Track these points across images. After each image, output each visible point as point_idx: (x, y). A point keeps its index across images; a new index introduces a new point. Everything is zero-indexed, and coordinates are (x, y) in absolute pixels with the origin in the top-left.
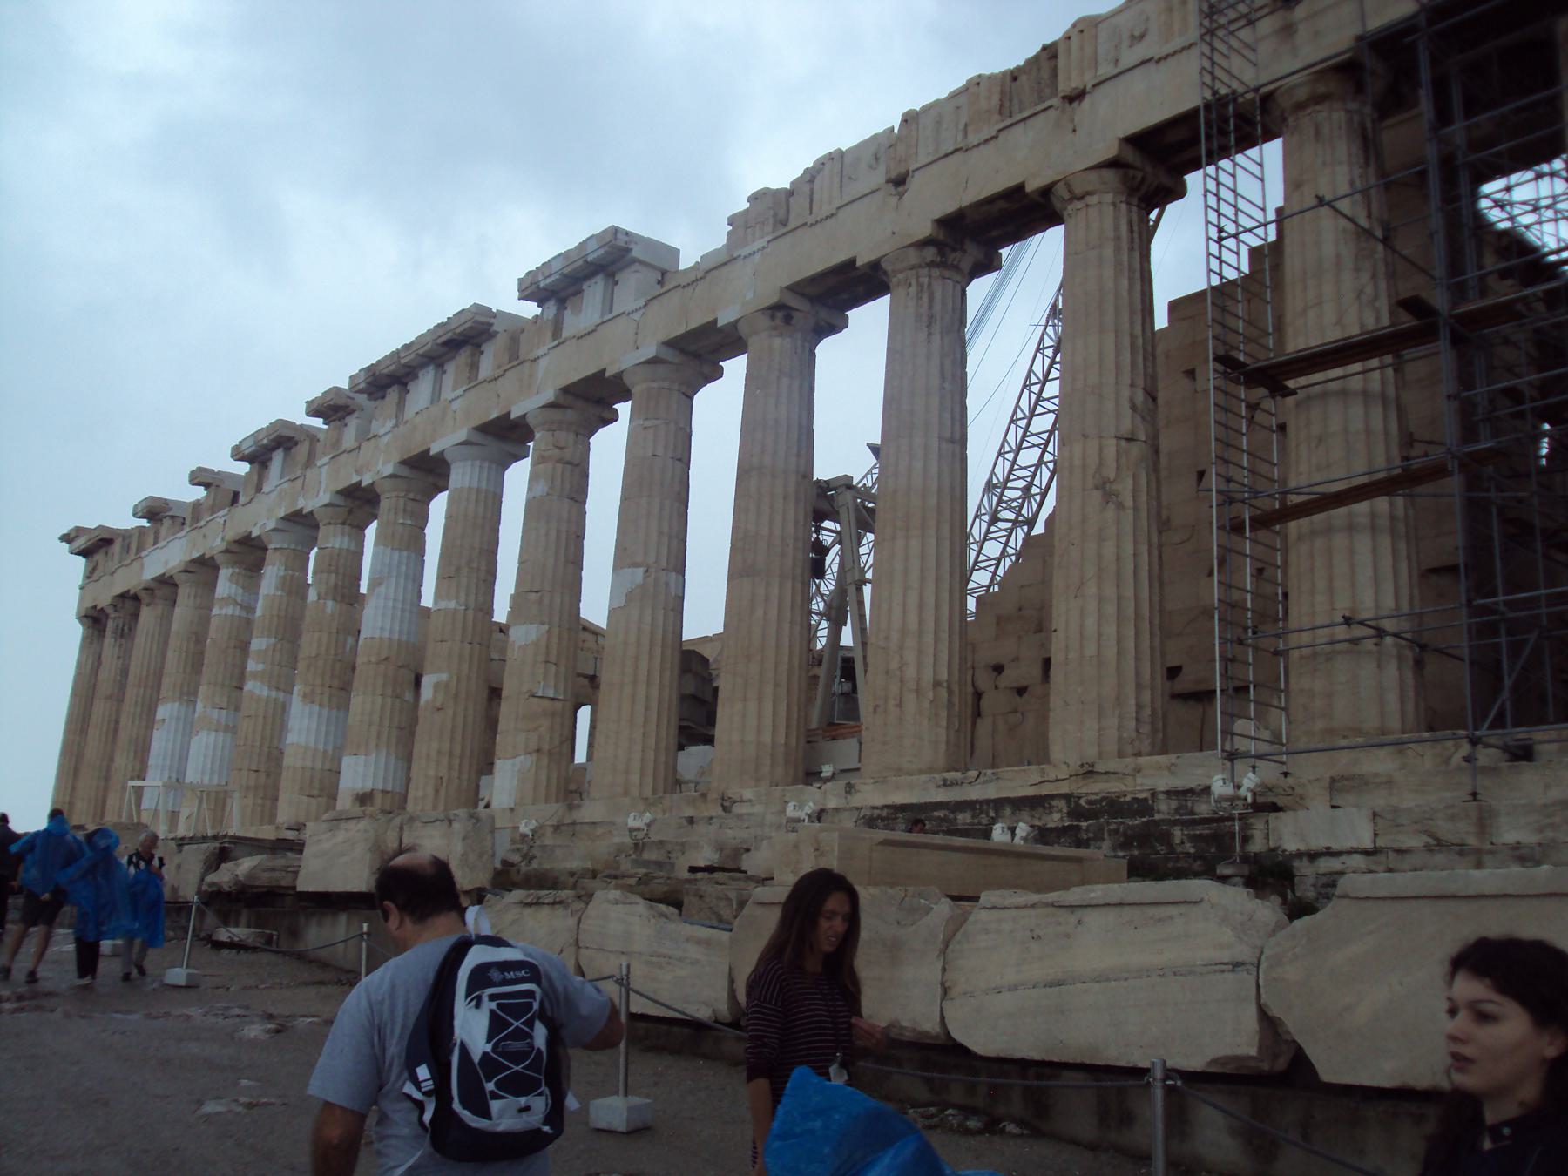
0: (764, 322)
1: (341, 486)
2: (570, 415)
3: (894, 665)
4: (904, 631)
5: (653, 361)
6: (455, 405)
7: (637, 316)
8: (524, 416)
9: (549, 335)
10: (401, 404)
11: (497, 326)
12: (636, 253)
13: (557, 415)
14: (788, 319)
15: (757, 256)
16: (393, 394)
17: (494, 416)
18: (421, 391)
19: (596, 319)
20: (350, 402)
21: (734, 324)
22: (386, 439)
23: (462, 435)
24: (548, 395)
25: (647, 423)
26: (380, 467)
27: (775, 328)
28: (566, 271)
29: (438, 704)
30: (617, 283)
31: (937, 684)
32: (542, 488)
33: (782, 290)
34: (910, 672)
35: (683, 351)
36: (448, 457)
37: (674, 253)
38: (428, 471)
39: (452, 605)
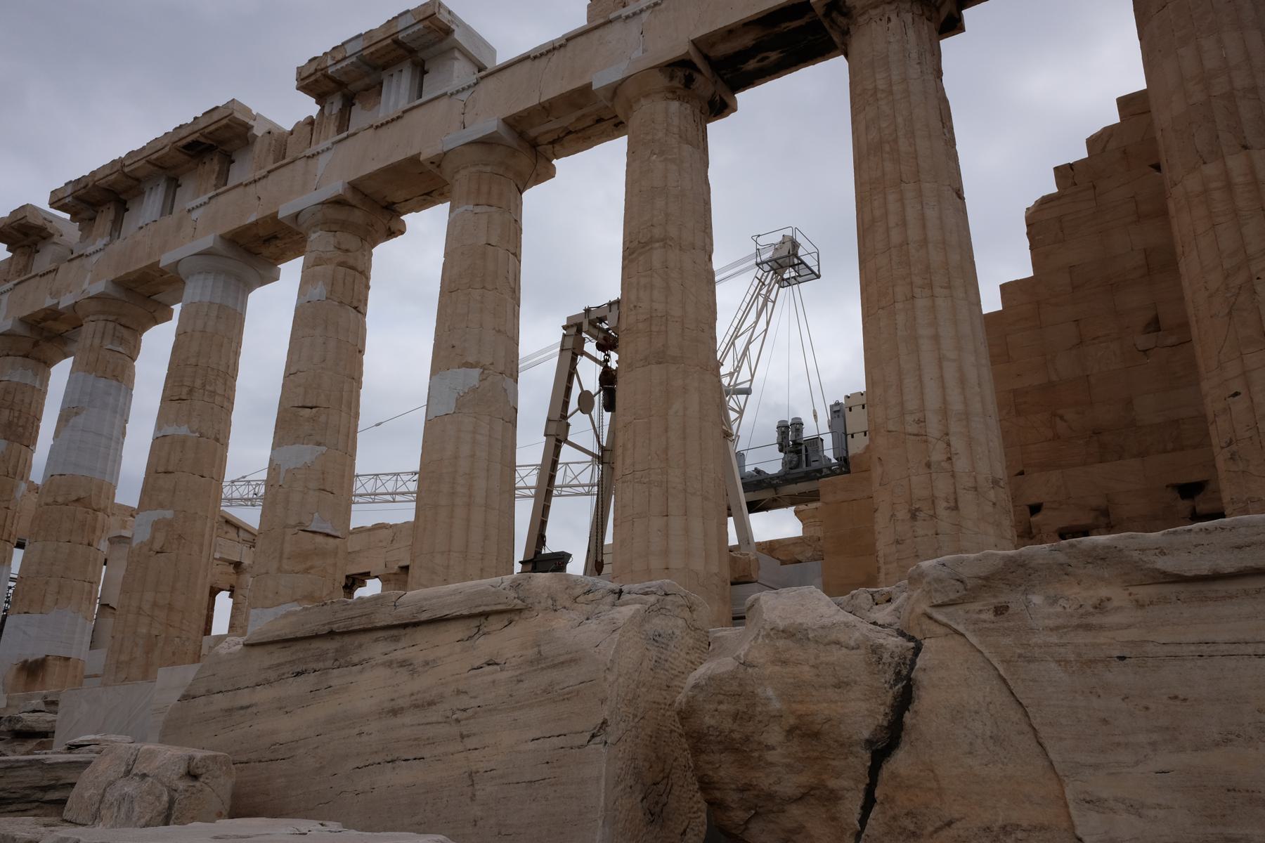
0: (661, 81)
1: (26, 312)
2: (358, 216)
3: (937, 456)
4: (944, 412)
5: (486, 142)
6: (194, 215)
7: (464, 96)
8: (297, 215)
9: (333, 128)
10: (117, 223)
11: (258, 131)
12: (458, 35)
13: (341, 214)
14: (689, 81)
15: (645, 16)
16: (105, 219)
17: (252, 218)
18: (149, 207)
19: (404, 104)
20: (48, 225)
21: (615, 90)
22: (94, 259)
23: (207, 241)
24: (335, 187)
25: (478, 209)
26: (85, 286)
27: (673, 91)
28: (365, 53)
29: (157, 547)
30: (426, 72)
31: (995, 482)
32: (319, 291)
33: (695, 43)
34: (961, 464)
35: (521, 135)
36: (182, 269)
37: (492, 52)
38: (143, 296)
39: (183, 430)
